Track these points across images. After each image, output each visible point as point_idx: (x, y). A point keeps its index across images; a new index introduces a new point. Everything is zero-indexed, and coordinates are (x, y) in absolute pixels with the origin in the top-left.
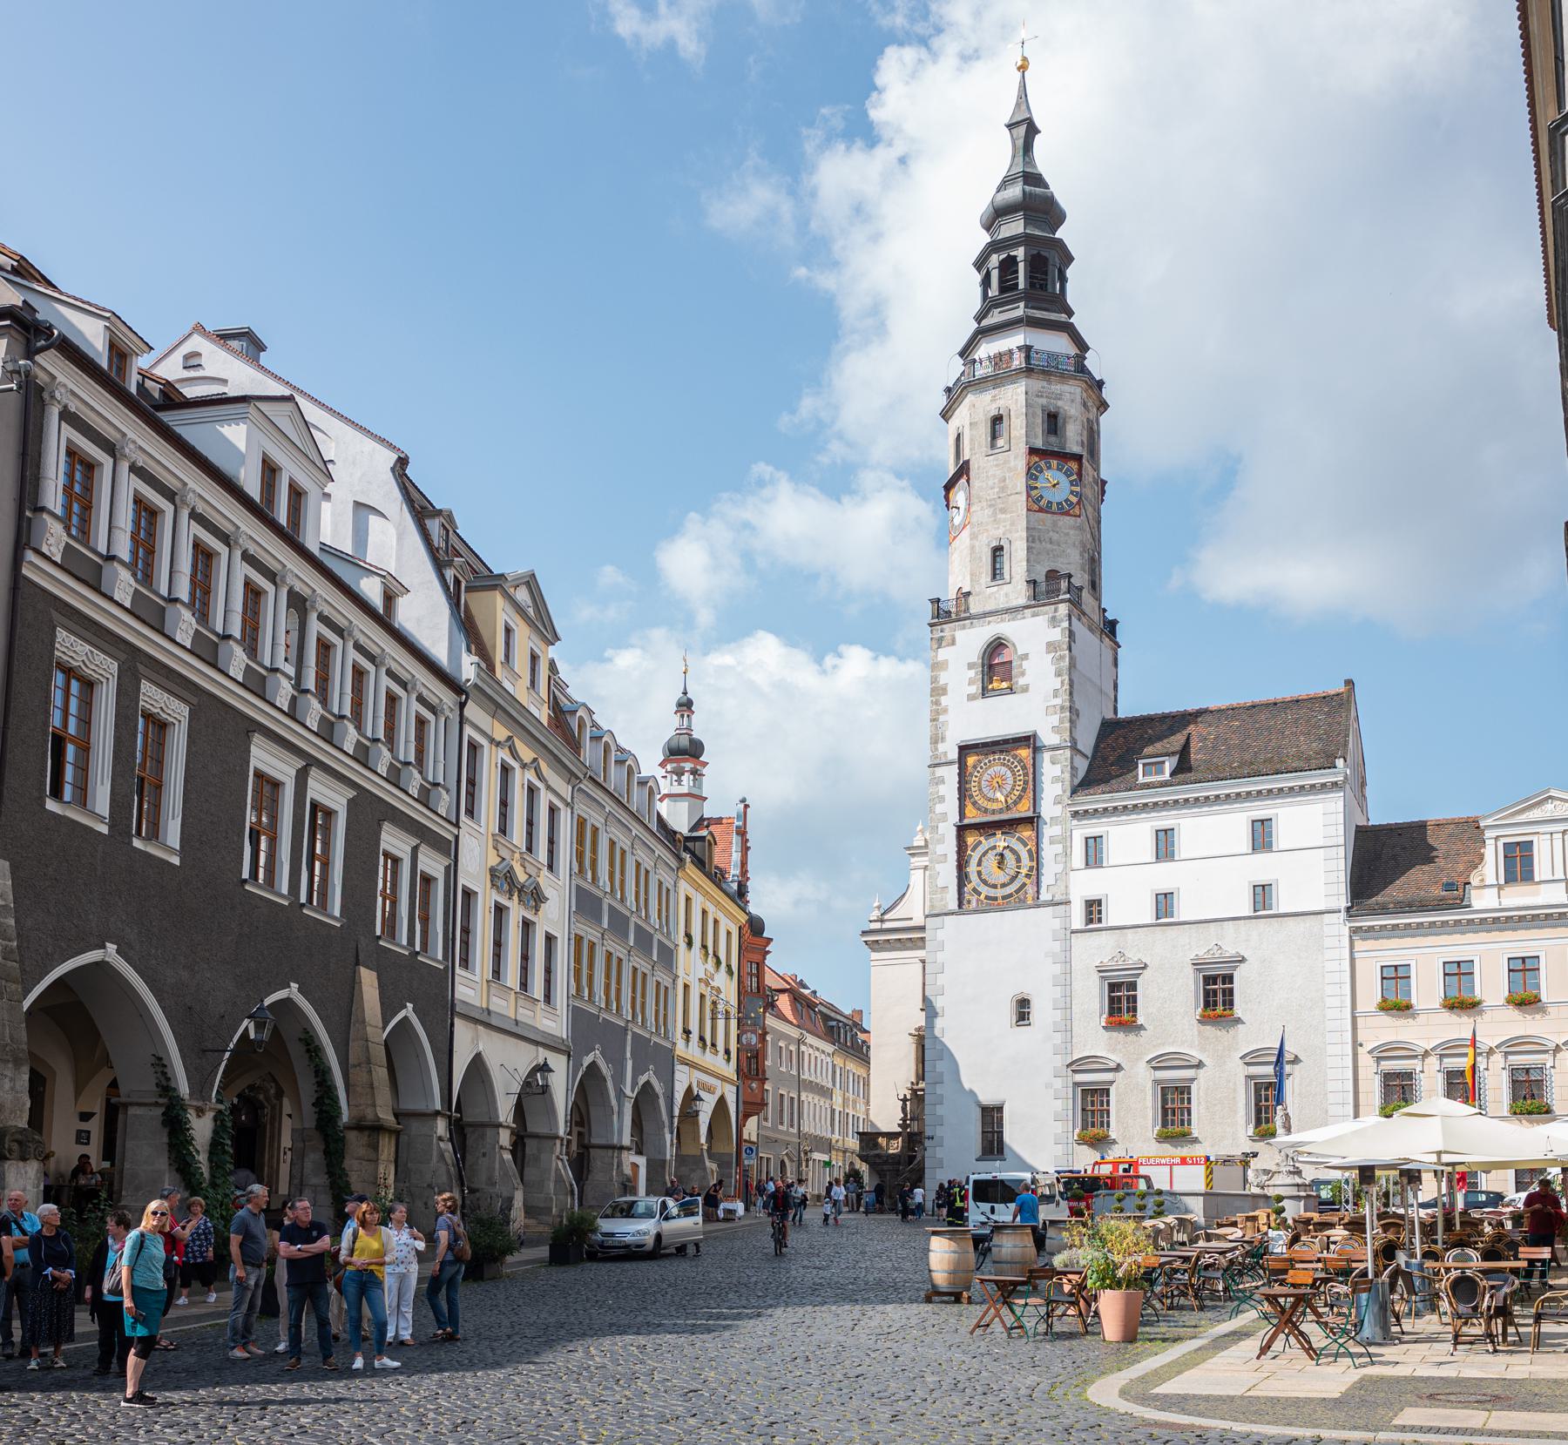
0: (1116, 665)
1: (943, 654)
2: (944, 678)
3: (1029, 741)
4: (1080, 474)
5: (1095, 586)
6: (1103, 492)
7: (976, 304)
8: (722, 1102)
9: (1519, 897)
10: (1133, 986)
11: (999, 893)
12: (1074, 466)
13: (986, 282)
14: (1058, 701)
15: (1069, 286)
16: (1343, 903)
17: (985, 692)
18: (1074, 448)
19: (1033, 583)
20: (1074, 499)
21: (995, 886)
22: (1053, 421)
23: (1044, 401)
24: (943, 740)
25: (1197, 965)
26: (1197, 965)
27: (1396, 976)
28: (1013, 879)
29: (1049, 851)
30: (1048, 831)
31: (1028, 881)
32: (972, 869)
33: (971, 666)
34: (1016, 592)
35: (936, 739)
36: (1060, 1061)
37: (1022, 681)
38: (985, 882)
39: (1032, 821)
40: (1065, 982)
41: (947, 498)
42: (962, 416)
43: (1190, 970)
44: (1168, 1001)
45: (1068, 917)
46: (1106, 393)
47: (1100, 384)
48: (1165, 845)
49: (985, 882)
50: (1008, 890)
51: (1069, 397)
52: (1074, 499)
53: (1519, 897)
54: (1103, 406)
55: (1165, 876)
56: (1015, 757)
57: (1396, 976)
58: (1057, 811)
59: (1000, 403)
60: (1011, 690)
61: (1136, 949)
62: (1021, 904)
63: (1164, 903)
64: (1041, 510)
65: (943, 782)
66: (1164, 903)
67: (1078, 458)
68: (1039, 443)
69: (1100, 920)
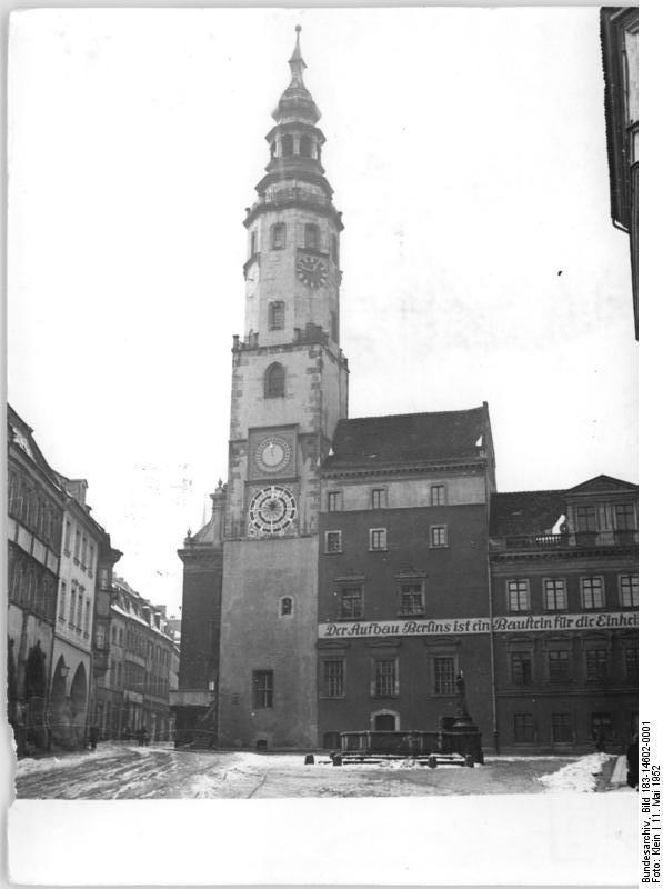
1: (241, 370)
5: (336, 338)
7: (267, 160)
8: (81, 666)
13: (273, 149)
14: (314, 404)
15: (322, 155)
31: (291, 520)
35: (234, 425)
41: (245, 274)
42: (257, 223)
46: (344, 220)
54: (341, 227)
59: (281, 220)
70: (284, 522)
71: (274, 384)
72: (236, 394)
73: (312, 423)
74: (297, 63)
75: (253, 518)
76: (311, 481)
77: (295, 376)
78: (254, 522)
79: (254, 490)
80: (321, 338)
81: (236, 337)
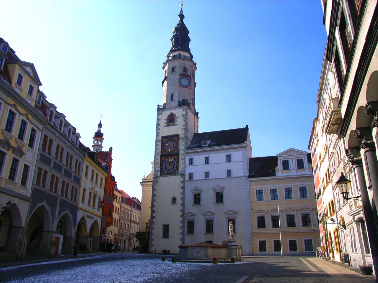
0: (198, 122)
1: (160, 117)
2: (160, 122)
3: (177, 136)
4: (190, 80)
5: (194, 104)
6: (196, 85)
9: (286, 174)
10: (199, 195)
11: (169, 172)
12: (189, 78)
14: (184, 127)
16: (247, 175)
17: (168, 125)
18: (189, 75)
19: (179, 102)
20: (189, 85)
21: (168, 170)
22: (185, 69)
23: (183, 65)
24: (159, 136)
25: (214, 189)
26: (214, 189)
27: (260, 192)
28: (173, 169)
29: (181, 162)
30: (181, 157)
31: (176, 169)
32: (164, 166)
33: (165, 119)
34: (175, 103)
35: (157, 135)
36: (181, 213)
37: (176, 123)
38: (166, 169)
39: (177, 154)
40: (183, 193)
43: (212, 191)
44: (208, 197)
45: (184, 178)
46: (197, 66)
47: (195, 64)
48: (207, 160)
49: (166, 169)
50: (172, 171)
51: (187, 64)
52: (189, 85)
53: (286, 174)
54: (196, 68)
55: (207, 168)
56: (174, 140)
57: (260, 192)
58: (183, 152)
59: (174, 65)
60: (174, 125)
61: (200, 186)
62: (175, 174)
63: (207, 174)
64: (182, 87)
65: (158, 146)
66: (207, 174)
67: (190, 77)
68: (182, 73)
69: (192, 179)
70: (173, 170)
71: (171, 120)
72: (158, 125)
73: (183, 134)
74: (182, 16)
75: (163, 169)
76: (182, 155)
77: (178, 117)
78: (163, 170)
79: (164, 158)
80: (187, 103)
81: (158, 105)
